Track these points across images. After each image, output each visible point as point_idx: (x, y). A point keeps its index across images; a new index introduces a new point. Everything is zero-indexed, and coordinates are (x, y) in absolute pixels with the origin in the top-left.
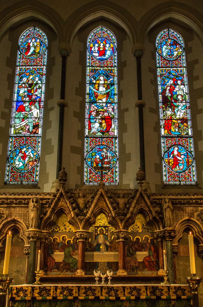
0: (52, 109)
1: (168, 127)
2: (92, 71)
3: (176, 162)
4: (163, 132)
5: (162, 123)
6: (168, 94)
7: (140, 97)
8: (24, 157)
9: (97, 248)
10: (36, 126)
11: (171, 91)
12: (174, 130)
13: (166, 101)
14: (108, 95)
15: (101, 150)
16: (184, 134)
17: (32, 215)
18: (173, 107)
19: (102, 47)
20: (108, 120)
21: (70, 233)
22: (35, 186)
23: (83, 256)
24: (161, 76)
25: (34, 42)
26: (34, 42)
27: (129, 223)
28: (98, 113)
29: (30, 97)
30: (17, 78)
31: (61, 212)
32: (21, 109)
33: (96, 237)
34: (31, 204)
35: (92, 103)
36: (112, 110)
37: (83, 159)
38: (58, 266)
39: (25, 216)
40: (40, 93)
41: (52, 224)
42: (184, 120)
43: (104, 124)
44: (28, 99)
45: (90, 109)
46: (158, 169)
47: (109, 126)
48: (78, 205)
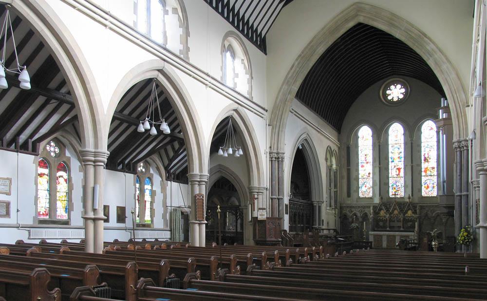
0: (376, 167)
1: (425, 171)
2: (392, 147)
3: (428, 187)
4: (423, 174)
5: (423, 170)
6: (426, 156)
7: (412, 163)
8: (366, 187)
9: (394, 221)
10: (369, 174)
11: (428, 154)
12: (428, 173)
13: (425, 160)
14: (399, 157)
15: (396, 182)
16: (432, 174)
17: (372, 211)
18: (428, 161)
19: (396, 132)
20: (399, 169)
21: (385, 217)
22: (371, 198)
23: (389, 224)
24: (424, 146)
25: (365, 134)
26: (365, 134)
27: (406, 212)
28: (395, 167)
29: (366, 160)
30: (360, 152)
31: (381, 209)
32: (362, 166)
33: (394, 218)
34: (371, 208)
35: (392, 162)
36: (401, 165)
37: (389, 187)
38: (381, 227)
39: (370, 211)
40: (370, 159)
41: (378, 213)
42: (433, 168)
43: (398, 172)
44: (365, 162)
45: (391, 165)
46: (420, 190)
47: (399, 172)
48: (387, 208)
